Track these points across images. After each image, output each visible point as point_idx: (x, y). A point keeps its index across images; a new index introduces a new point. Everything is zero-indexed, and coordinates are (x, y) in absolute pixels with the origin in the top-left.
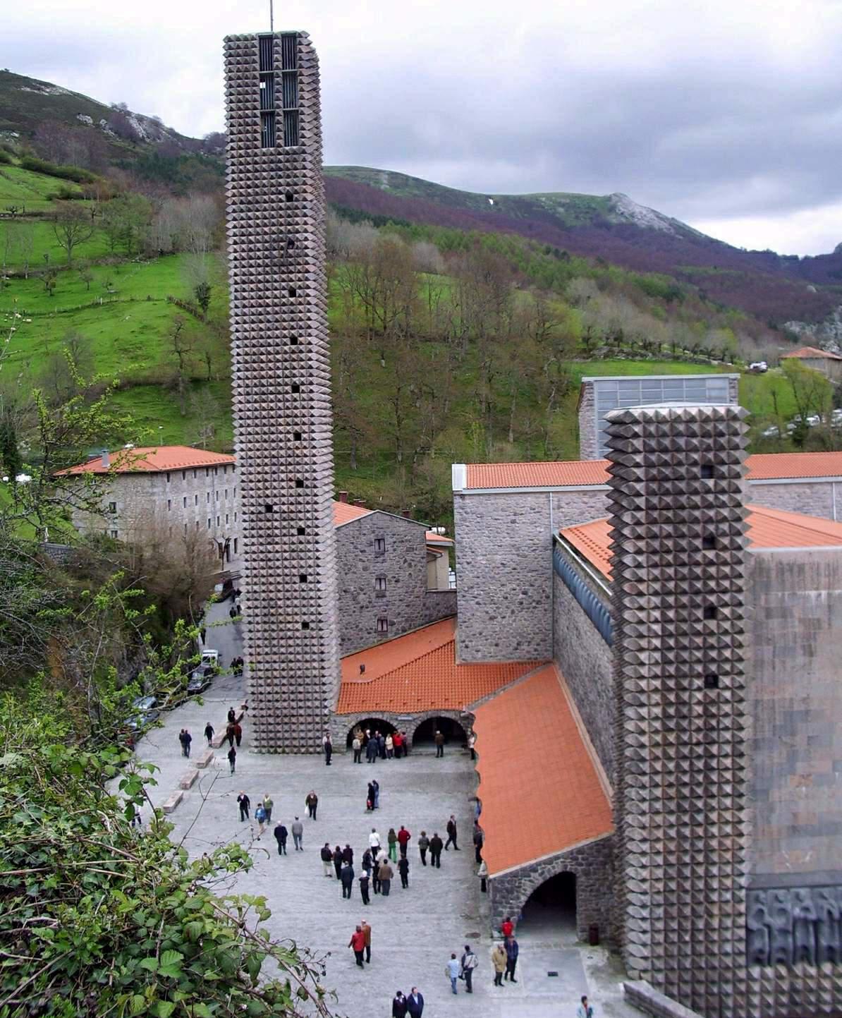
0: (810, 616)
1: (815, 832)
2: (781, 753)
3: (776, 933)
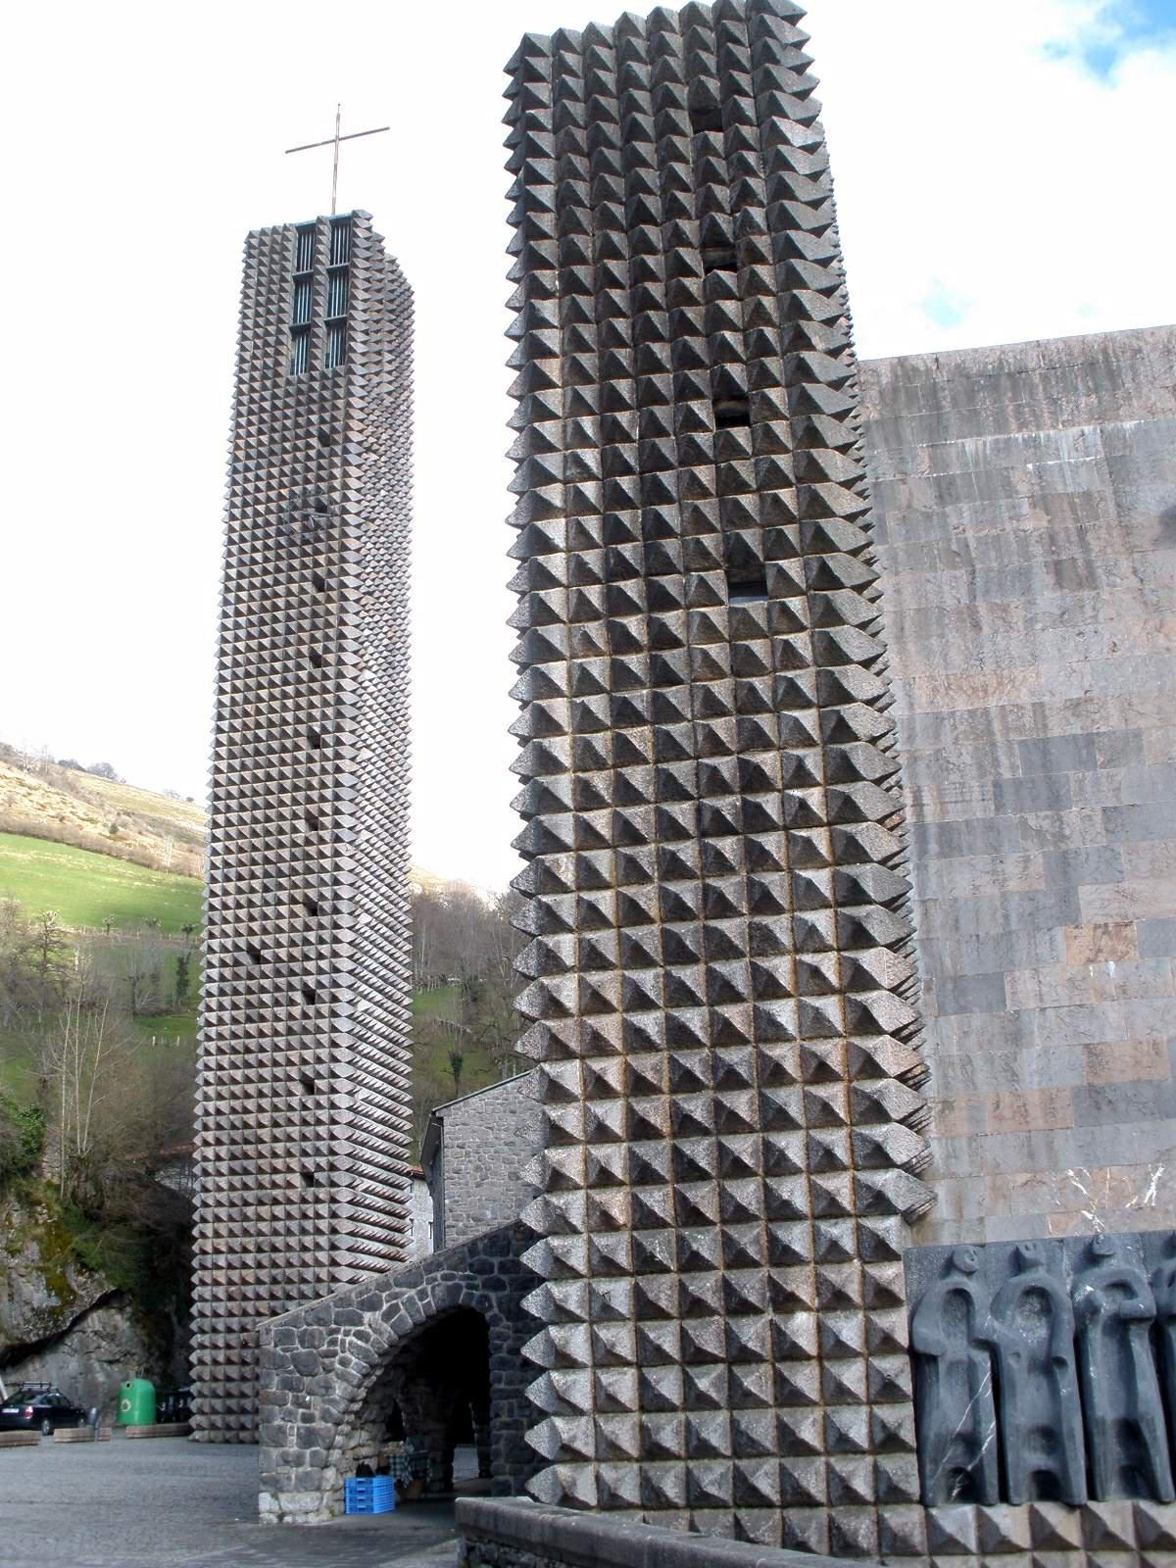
0: (1060, 489)
2: (1027, 860)
3: (1010, 1362)
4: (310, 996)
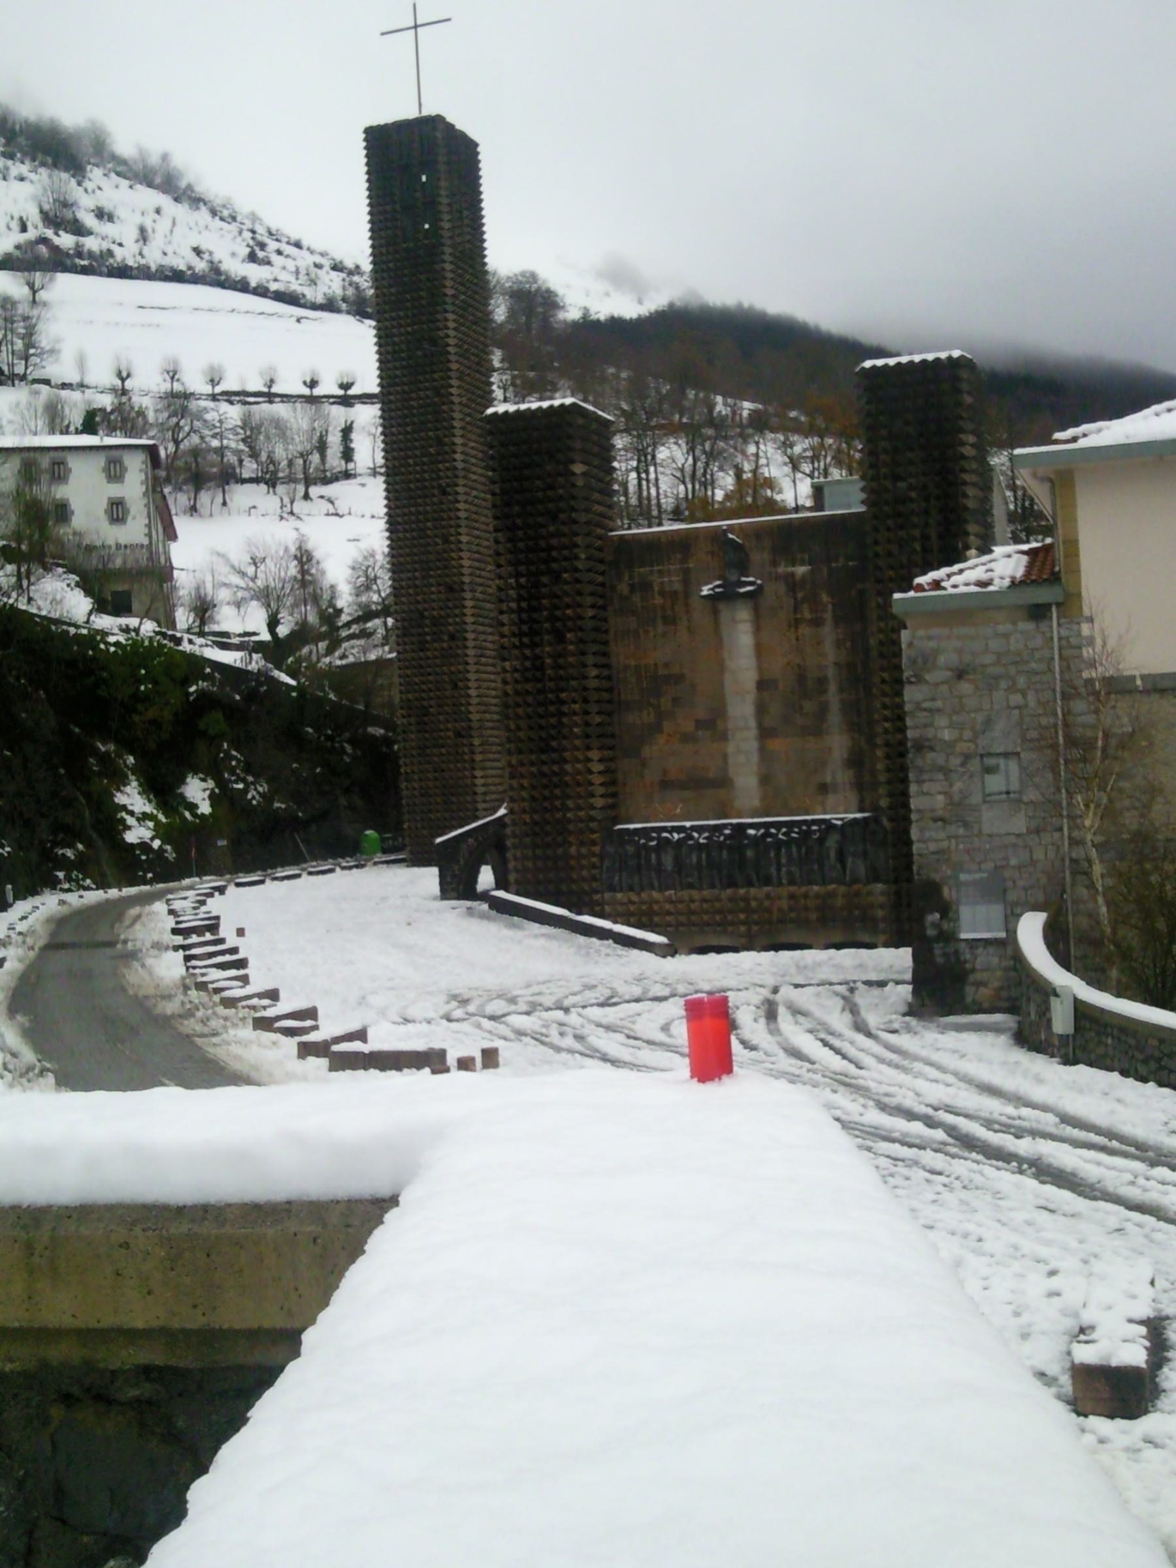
1: (683, 786)
4: (452, 637)
